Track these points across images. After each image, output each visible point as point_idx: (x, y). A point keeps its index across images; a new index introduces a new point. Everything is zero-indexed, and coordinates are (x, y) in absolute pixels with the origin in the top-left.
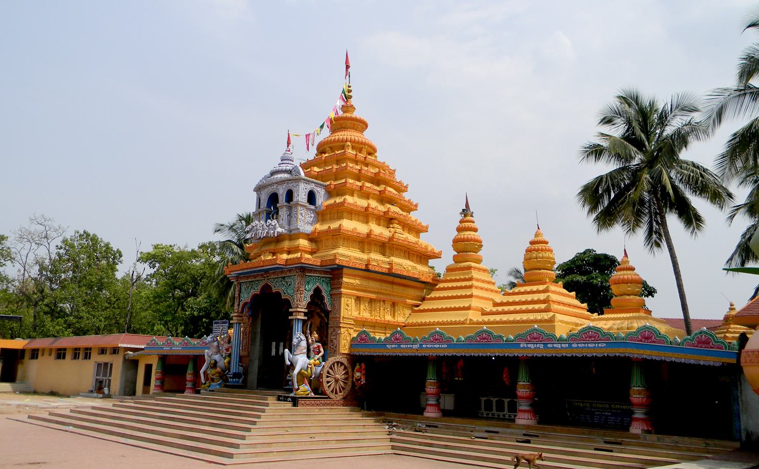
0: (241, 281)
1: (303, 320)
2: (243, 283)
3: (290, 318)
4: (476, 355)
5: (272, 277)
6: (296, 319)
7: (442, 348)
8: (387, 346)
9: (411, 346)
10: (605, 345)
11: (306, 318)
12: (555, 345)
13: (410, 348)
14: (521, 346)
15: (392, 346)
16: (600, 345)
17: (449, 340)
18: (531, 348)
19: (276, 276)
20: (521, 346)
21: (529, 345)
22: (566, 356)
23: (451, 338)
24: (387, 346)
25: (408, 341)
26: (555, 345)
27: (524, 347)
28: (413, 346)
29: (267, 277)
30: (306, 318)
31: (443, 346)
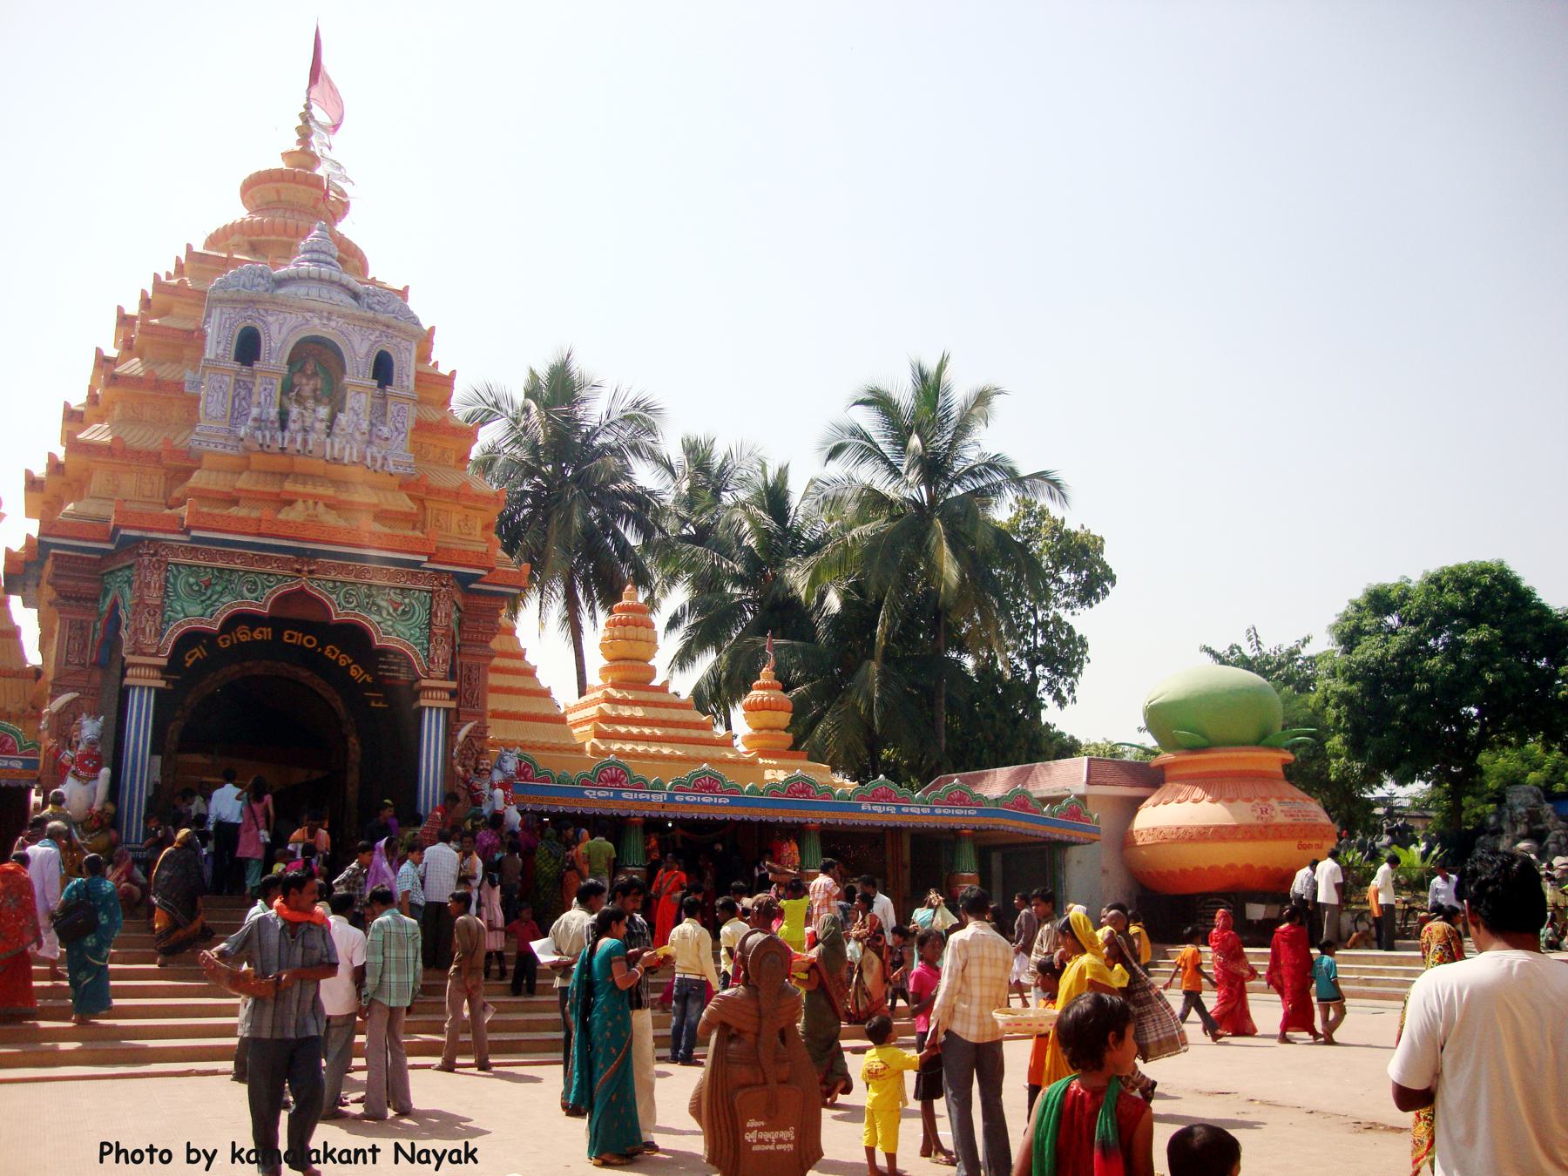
0: (171, 559)
1: (447, 710)
2: (176, 565)
3: (423, 702)
4: (788, 820)
5: (332, 576)
6: (431, 708)
7: (718, 804)
8: (586, 792)
9: (648, 796)
10: (975, 812)
11: (453, 704)
12: (912, 809)
13: (645, 800)
14: (863, 808)
15: (599, 794)
16: (970, 812)
17: (734, 791)
18: (876, 812)
19: (353, 579)
20: (863, 808)
21: (874, 808)
22: (843, 824)
23: (737, 786)
24: (586, 792)
25: (640, 785)
26: (912, 809)
27: (867, 811)
28: (653, 796)
29: (311, 572)
30: (453, 704)
31: (720, 801)
